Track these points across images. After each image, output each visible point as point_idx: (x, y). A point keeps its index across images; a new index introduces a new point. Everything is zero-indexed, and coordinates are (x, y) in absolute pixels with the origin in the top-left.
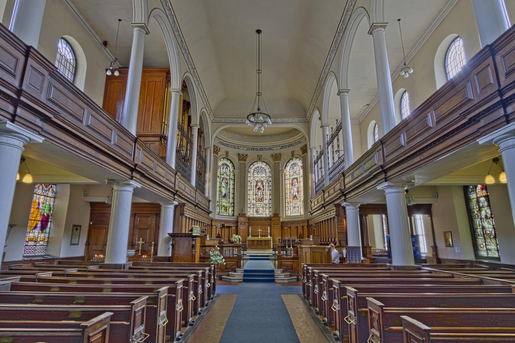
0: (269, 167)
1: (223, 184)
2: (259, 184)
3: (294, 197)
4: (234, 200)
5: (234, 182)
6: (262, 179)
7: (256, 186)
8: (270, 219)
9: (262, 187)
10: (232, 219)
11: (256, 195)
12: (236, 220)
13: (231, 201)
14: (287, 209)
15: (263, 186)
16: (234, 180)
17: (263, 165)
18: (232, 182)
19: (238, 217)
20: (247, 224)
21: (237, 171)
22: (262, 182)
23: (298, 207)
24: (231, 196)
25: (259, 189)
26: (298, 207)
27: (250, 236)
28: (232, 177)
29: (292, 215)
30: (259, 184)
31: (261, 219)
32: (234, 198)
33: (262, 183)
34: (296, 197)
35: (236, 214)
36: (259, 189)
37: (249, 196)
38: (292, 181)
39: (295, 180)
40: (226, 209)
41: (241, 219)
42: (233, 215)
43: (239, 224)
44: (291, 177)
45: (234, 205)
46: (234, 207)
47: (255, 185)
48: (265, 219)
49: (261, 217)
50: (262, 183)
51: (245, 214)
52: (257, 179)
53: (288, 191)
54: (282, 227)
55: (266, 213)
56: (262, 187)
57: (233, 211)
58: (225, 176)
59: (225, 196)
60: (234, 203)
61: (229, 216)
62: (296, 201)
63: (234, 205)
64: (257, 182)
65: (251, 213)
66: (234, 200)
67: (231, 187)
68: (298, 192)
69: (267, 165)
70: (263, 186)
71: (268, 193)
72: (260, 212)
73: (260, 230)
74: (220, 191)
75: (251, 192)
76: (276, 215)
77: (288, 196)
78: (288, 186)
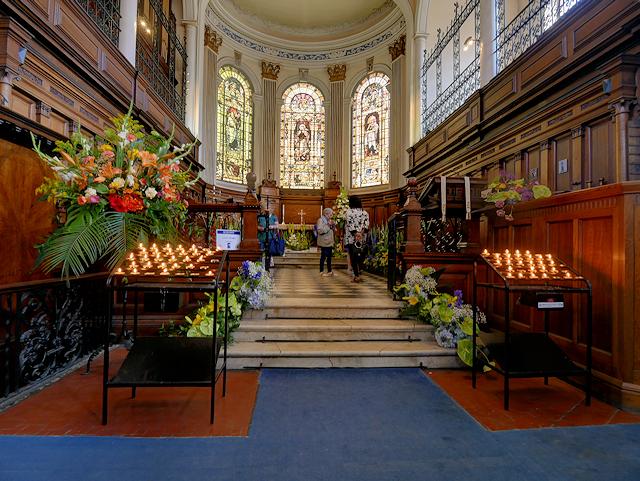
1: (231, 121)
2: (302, 127)
3: (369, 151)
5: (253, 119)
6: (309, 119)
7: (296, 131)
8: (321, 192)
9: (306, 134)
13: (247, 156)
14: (354, 175)
15: (309, 132)
16: (253, 116)
17: (310, 90)
18: (248, 119)
20: (278, 201)
24: (248, 147)
25: (302, 136)
28: (248, 108)
29: (363, 185)
30: (302, 127)
32: (252, 151)
33: (307, 126)
36: (302, 136)
38: (366, 120)
39: (373, 117)
40: (236, 171)
41: (266, 191)
44: (366, 113)
46: (252, 168)
47: (294, 128)
48: (313, 192)
50: (307, 126)
52: (297, 118)
53: (357, 141)
56: (306, 134)
59: (234, 145)
63: (252, 164)
64: (298, 123)
65: (286, 181)
66: (252, 155)
67: (248, 128)
68: (377, 141)
70: (309, 132)
71: (320, 144)
72: (304, 181)
74: (224, 133)
75: (287, 142)
76: (334, 186)
77: (357, 150)
78: (358, 131)
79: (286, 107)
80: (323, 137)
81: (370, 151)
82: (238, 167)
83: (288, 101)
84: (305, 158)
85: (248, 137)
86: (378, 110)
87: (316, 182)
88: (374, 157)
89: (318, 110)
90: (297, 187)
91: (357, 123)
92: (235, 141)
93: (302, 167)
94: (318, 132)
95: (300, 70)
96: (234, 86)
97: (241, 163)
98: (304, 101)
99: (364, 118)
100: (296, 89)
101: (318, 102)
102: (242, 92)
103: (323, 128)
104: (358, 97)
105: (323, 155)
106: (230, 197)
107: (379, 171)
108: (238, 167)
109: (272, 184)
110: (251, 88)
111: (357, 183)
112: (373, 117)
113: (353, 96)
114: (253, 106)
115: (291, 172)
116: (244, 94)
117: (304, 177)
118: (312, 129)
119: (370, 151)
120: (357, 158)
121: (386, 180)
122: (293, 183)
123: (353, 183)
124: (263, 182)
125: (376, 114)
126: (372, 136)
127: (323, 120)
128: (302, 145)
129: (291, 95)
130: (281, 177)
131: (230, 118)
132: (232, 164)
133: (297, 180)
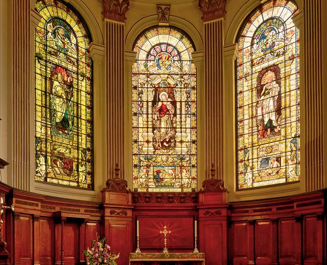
0: (188, 45)
1: (58, 88)
2: (163, 96)
3: (265, 129)
4: (92, 142)
5: (92, 85)
6: (172, 82)
7: (155, 102)
8: (194, 196)
9: (169, 106)
10: (86, 197)
11: (154, 129)
12: (99, 201)
13: (84, 143)
14: (241, 169)
15: (174, 103)
16: (91, 80)
17: (174, 39)
19: (103, 192)
20: (130, 213)
21: (99, 52)
22: (171, 90)
23: (278, 160)
24: (84, 128)
25: (163, 111)
26: (278, 160)
27: (138, 251)
28: (84, 69)
29: (256, 185)
30: (163, 96)
31: (170, 197)
32: (91, 136)
33: (171, 95)
34: (273, 128)
35: (100, 182)
36: (163, 111)
37: (135, 132)
38: (259, 79)
39: (270, 75)
40: (69, 167)
41: (111, 198)
42: (91, 187)
43: (107, 212)
44: (258, 68)
45: (92, 155)
46: (92, 162)
47: (151, 98)
48: (182, 197)
49: (168, 193)
50: (171, 95)
51: (125, 183)
52: (156, 82)
53: (245, 114)
54: (230, 223)
55: (183, 180)
56: (169, 106)
57: (92, 174)
58: (60, 60)
59: (64, 125)
60: (91, 150)
61: (78, 187)
62: (270, 140)
63: (92, 155)
64: (157, 90)
66: (92, 142)
67: (84, 99)
69: (185, 40)
70: (174, 103)
71: (189, 122)
73: (165, 232)
74: (49, 108)
75: (141, 121)
76: (213, 185)
77: (246, 128)
78: (247, 98)
79: (139, 67)
80: (194, 111)
81: (268, 129)
82: (71, 162)
83: (142, 55)
84: (169, 143)
85: (84, 113)
86: (276, 61)
87: (185, 181)
88: (273, 139)
89: (186, 69)
90: (157, 190)
91: (245, 85)
92: (65, 121)
93: (164, 158)
94: (187, 102)
95: (158, 7)
96: (61, 31)
97: (75, 153)
98: (165, 56)
99: (255, 76)
100: (154, 39)
101: (186, 56)
102: (74, 41)
103: (193, 97)
104: (246, 42)
105: (194, 138)
106: (57, 209)
107: (283, 160)
108: (71, 162)
109: (117, 184)
110: (88, 36)
111: (247, 180)
112: (270, 75)
113: (237, 41)
114: (91, 66)
115: (148, 166)
116: (77, 45)
117: (167, 173)
118: (178, 99)
119: (268, 129)
120: (245, 141)
121: (293, 172)
122: (152, 184)
123: (241, 182)
124: (108, 184)
125: (275, 69)
126: (270, 104)
127: (193, 84)
128: (163, 126)
129: (147, 46)
130: (135, 174)
131: (56, 83)
132: (61, 157)
133: (158, 179)
